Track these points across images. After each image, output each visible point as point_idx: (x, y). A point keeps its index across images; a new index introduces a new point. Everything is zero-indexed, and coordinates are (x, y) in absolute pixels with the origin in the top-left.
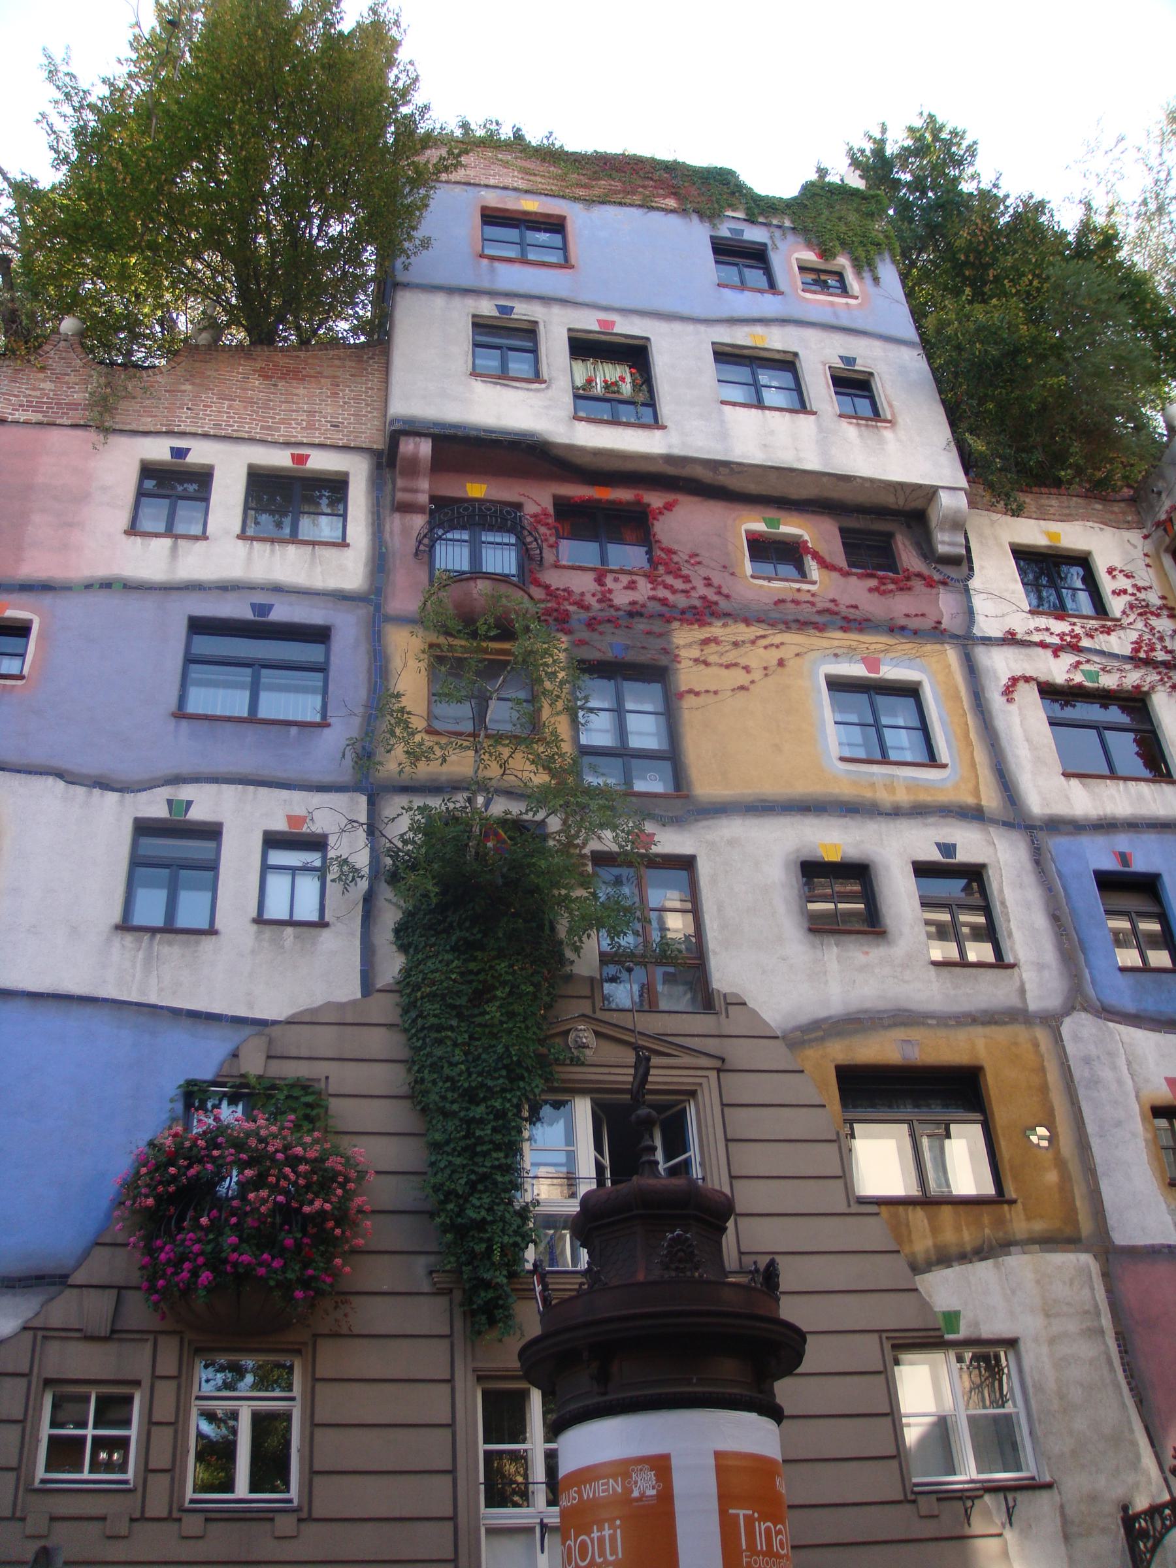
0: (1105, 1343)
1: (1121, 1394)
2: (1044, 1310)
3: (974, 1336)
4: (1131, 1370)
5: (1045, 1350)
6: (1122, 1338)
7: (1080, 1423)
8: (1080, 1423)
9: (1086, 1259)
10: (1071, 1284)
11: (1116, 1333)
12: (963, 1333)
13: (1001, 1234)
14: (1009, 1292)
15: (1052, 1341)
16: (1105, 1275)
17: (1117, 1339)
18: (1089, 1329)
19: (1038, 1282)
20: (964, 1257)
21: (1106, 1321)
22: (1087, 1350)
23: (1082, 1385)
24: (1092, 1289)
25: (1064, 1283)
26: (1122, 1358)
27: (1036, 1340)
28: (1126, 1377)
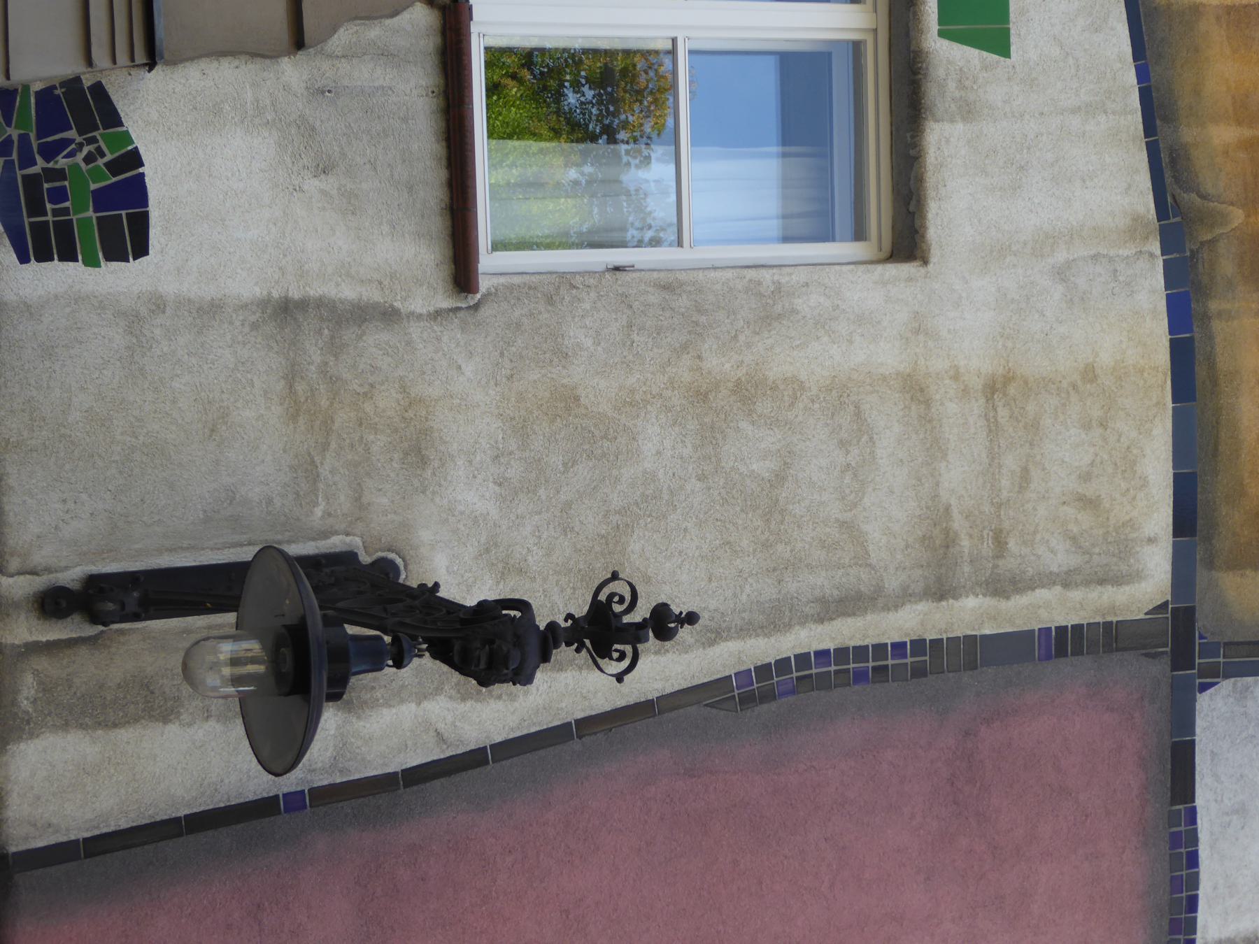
0: (905, 597)
1: (746, 630)
2: (1008, 379)
3: (932, 92)
4: (823, 682)
5: (889, 357)
6: (924, 661)
7: (658, 445)
8: (658, 445)
9: (1150, 581)
10: (1089, 503)
11: (936, 643)
12: (947, 57)
13: (1227, 266)
14: (1061, 256)
15: (914, 389)
16: (1106, 639)
17: (919, 645)
18: (950, 540)
19: (1089, 374)
20: (1156, 110)
21: (971, 614)
22: (888, 523)
23: (780, 478)
24: (1067, 580)
25: (1086, 477)
26: (861, 652)
27: (919, 328)
28: (803, 659)
